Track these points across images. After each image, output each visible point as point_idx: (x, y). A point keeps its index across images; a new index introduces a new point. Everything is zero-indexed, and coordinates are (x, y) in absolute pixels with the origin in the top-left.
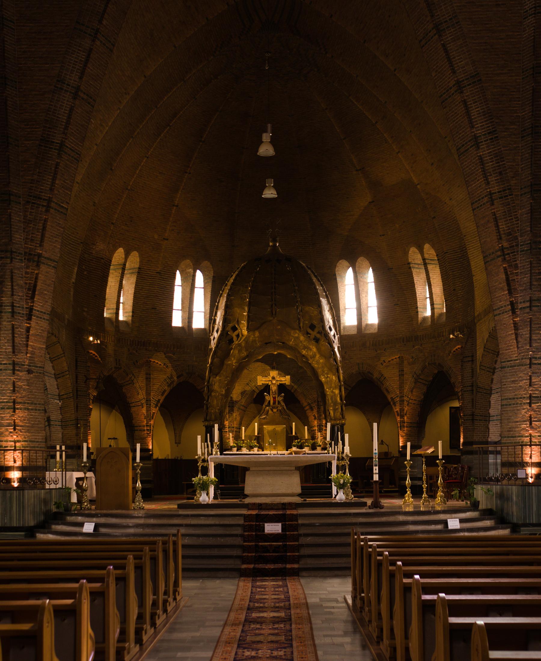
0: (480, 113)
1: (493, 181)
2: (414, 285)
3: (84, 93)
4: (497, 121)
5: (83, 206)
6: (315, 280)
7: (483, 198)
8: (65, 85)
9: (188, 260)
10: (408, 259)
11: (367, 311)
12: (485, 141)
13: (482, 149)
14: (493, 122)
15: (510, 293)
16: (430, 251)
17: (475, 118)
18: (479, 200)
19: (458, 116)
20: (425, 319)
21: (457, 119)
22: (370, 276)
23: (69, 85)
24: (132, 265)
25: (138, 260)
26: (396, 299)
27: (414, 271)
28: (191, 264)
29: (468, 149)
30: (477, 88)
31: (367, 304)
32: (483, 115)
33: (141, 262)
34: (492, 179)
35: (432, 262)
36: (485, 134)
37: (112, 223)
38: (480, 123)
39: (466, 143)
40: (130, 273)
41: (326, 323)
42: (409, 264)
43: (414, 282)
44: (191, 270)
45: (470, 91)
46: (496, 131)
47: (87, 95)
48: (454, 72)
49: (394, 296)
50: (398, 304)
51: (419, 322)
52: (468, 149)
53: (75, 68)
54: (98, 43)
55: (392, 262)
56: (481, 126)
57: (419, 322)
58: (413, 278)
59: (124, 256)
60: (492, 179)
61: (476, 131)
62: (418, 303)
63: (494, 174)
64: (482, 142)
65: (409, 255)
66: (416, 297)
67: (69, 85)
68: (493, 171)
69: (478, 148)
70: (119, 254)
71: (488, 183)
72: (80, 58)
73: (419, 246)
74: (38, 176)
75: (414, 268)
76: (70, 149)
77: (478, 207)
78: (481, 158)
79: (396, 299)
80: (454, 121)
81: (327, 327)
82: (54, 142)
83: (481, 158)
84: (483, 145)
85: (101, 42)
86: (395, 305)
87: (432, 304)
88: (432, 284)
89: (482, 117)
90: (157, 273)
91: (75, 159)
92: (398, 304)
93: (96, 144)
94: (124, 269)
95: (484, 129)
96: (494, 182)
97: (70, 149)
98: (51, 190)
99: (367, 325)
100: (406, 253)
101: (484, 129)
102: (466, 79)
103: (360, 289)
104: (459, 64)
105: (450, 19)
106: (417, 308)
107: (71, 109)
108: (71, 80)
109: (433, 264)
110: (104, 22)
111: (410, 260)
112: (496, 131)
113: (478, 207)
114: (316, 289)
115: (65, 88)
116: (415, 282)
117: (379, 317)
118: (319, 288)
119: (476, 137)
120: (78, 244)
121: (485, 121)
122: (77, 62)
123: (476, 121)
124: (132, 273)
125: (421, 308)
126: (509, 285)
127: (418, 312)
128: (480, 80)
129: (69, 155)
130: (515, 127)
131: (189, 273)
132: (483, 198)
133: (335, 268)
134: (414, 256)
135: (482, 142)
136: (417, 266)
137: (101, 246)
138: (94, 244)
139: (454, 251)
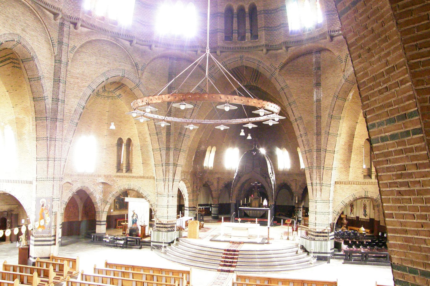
15: (311, 180)
34: (306, 147)
48: (294, 116)
54: (196, 107)
60: (306, 147)
69: (302, 138)
70: (209, 149)
71: (305, 148)
78: (302, 140)
83: (302, 140)
98: (181, 146)
119: (301, 135)
126: (311, 178)
137: (203, 147)
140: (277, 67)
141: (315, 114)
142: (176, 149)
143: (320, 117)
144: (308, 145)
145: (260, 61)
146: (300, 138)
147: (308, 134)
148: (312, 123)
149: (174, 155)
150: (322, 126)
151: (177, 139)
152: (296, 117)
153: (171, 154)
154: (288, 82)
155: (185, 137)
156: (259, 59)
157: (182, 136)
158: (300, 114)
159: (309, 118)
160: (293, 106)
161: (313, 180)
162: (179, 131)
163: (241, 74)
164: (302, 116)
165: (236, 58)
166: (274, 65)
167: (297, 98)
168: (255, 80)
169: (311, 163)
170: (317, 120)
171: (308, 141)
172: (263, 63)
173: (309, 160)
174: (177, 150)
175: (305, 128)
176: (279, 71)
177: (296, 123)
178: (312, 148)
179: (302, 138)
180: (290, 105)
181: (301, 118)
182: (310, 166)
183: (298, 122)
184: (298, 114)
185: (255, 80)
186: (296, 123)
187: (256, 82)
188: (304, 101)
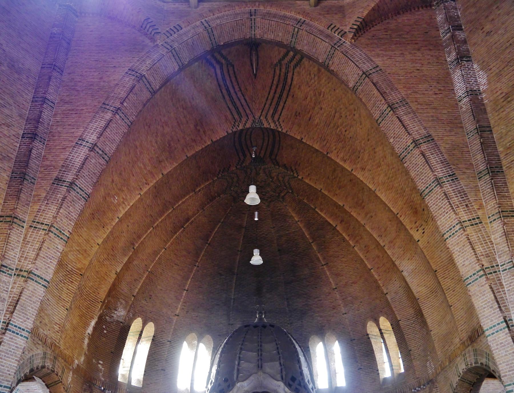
0: (438, 162)
1: (461, 211)
2: (374, 352)
3: (100, 149)
4: (454, 167)
5: (106, 272)
6: (294, 341)
7: (454, 227)
8: (85, 142)
9: (194, 334)
10: (366, 331)
11: (336, 376)
12: (447, 181)
13: (446, 187)
14: (451, 168)
16: (385, 323)
17: (435, 165)
18: (451, 229)
19: (419, 166)
20: (385, 379)
21: (418, 168)
22: (337, 347)
23: (88, 142)
24: (149, 334)
25: (153, 329)
26: (360, 365)
27: (373, 341)
28: (196, 337)
29: (433, 189)
30: (432, 145)
31: (335, 370)
32: (442, 163)
33: (156, 331)
35: (387, 332)
36: (446, 177)
37: (133, 296)
38: (440, 169)
39: (430, 185)
40: (146, 340)
41: (306, 377)
42: (368, 335)
43: (373, 350)
44: (196, 342)
45: (426, 147)
46: (454, 174)
47: (102, 151)
49: (357, 362)
50: (361, 369)
51: (381, 383)
52: (433, 189)
53: (95, 131)
55: (354, 335)
56: (441, 171)
57: (381, 383)
58: (372, 346)
59: (141, 325)
61: (438, 174)
62: (378, 366)
63: (461, 206)
64: (444, 182)
65: (367, 328)
66: (376, 362)
67: (88, 142)
68: (460, 204)
69: (442, 187)
72: (101, 125)
73: (375, 320)
74: (45, 206)
75: (372, 338)
76: (79, 188)
77: (450, 236)
79: (360, 365)
80: (416, 170)
81: (306, 381)
82: (65, 181)
84: (446, 184)
85: (120, 116)
86: (359, 369)
87: (391, 366)
88: (389, 349)
89: (441, 164)
90: (168, 341)
91: (83, 197)
92: (361, 369)
93: (118, 217)
94: (140, 335)
95: (444, 172)
96: (463, 212)
97: (79, 188)
99: (337, 388)
100: (364, 326)
101: (444, 172)
102: (421, 139)
103: (329, 358)
104: (413, 129)
105: (401, 102)
106: (378, 370)
107: (86, 159)
108: (90, 139)
109: (388, 334)
110: (125, 104)
111: (368, 332)
112: (454, 174)
113: (450, 236)
114: (296, 349)
115: (84, 144)
116: (374, 349)
117: (346, 381)
118: (299, 349)
120: (98, 302)
121: (444, 167)
122: (98, 127)
123: (436, 167)
124: (148, 340)
125: (381, 371)
127: (379, 374)
128: (433, 139)
129: (78, 193)
130: (471, 171)
131: (194, 344)
132: (454, 227)
133: (308, 342)
134: (372, 329)
135: (444, 182)
136: (374, 337)
137: (120, 313)
138: (116, 310)
139: (406, 318)
140: (347, 29)
141: (469, 125)
142: (35, 224)
143: (488, 129)
144: (467, 205)
145: (302, 21)
146: (438, 189)
147: (459, 177)
148: (466, 149)
149: (25, 242)
150: (500, 149)
151: (44, 195)
152: (417, 137)
153: (14, 237)
154: (378, 61)
155: (73, 193)
156: (299, 17)
157: (64, 189)
158: (425, 128)
159: (451, 138)
160: (401, 112)
161: (508, 310)
162: (55, 174)
163: (239, 94)
164: (432, 132)
165: (238, 14)
166: (338, 26)
167: (409, 92)
168: (273, 116)
169: (488, 256)
170: (481, 137)
171: (463, 194)
172: (308, 24)
173: (479, 249)
174: (39, 226)
175: (445, 163)
176: (352, 38)
177: (417, 152)
178: (480, 213)
179: (442, 187)
180: (392, 109)
181: (429, 138)
182: (486, 265)
183: (424, 147)
184: (420, 129)
185: (273, 116)
186: (417, 152)
187: (276, 117)
188: (431, 99)
